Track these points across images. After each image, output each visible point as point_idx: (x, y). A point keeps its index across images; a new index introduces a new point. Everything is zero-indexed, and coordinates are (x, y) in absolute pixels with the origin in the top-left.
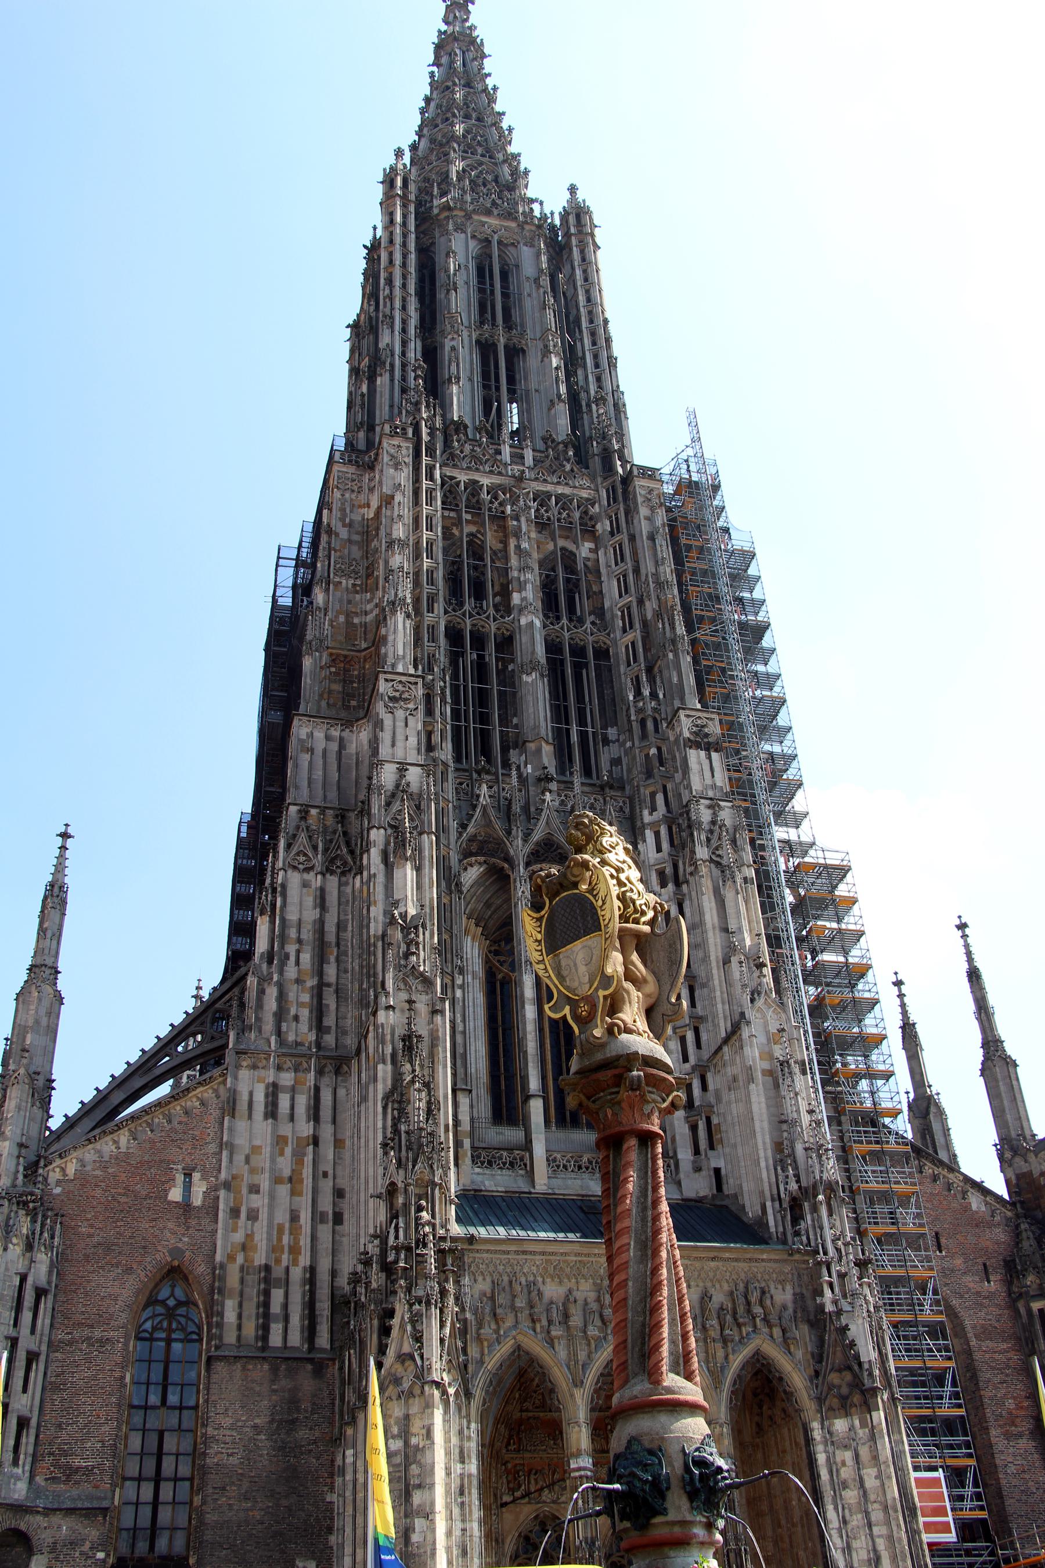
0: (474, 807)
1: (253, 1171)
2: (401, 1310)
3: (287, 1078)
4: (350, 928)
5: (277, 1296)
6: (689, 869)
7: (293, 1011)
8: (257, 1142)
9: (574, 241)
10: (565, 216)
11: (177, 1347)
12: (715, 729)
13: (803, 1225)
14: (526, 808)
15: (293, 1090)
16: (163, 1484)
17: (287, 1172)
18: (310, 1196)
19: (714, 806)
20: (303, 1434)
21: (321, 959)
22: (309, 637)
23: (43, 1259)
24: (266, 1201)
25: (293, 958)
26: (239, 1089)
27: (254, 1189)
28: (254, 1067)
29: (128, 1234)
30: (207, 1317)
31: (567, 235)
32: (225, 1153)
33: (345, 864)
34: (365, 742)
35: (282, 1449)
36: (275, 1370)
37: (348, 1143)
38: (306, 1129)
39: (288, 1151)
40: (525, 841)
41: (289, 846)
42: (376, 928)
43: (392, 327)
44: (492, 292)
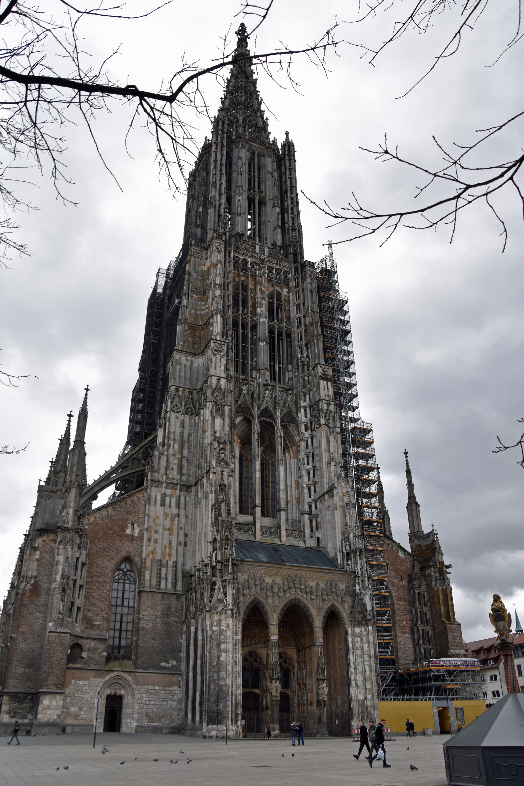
0: (240, 394)
1: (156, 525)
2: (219, 584)
3: (169, 492)
4: (193, 436)
5: (164, 570)
6: (317, 426)
7: (171, 466)
8: (158, 515)
9: (287, 158)
10: (283, 146)
11: (127, 586)
12: (330, 373)
13: (350, 562)
14: (259, 395)
15: (171, 496)
16: (122, 632)
17: (168, 526)
18: (176, 536)
19: (328, 404)
20: (172, 619)
21: (182, 447)
22: (180, 317)
23: (84, 553)
24: (161, 537)
25: (172, 446)
26: (152, 494)
27: (156, 532)
28: (158, 487)
29: (111, 545)
30: (138, 576)
31: (284, 153)
32: (146, 518)
33: (192, 411)
34: (201, 365)
35: (165, 624)
36: (163, 597)
37: (190, 517)
38: (175, 511)
39: (169, 518)
40: (259, 408)
41: (172, 402)
42: (207, 441)
43: (216, 188)
44: (254, 176)
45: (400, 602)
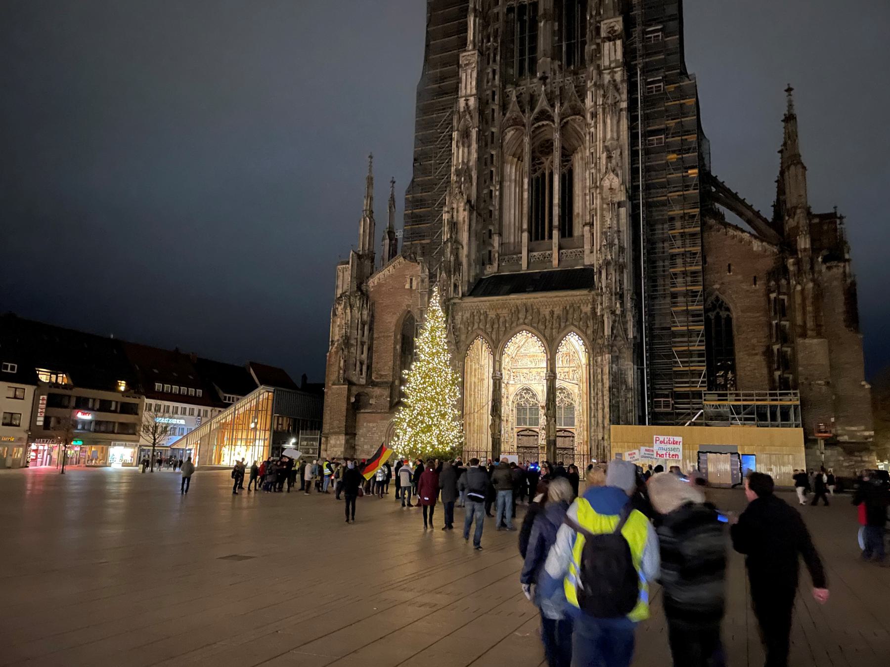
23: (365, 312)
45: (749, 314)
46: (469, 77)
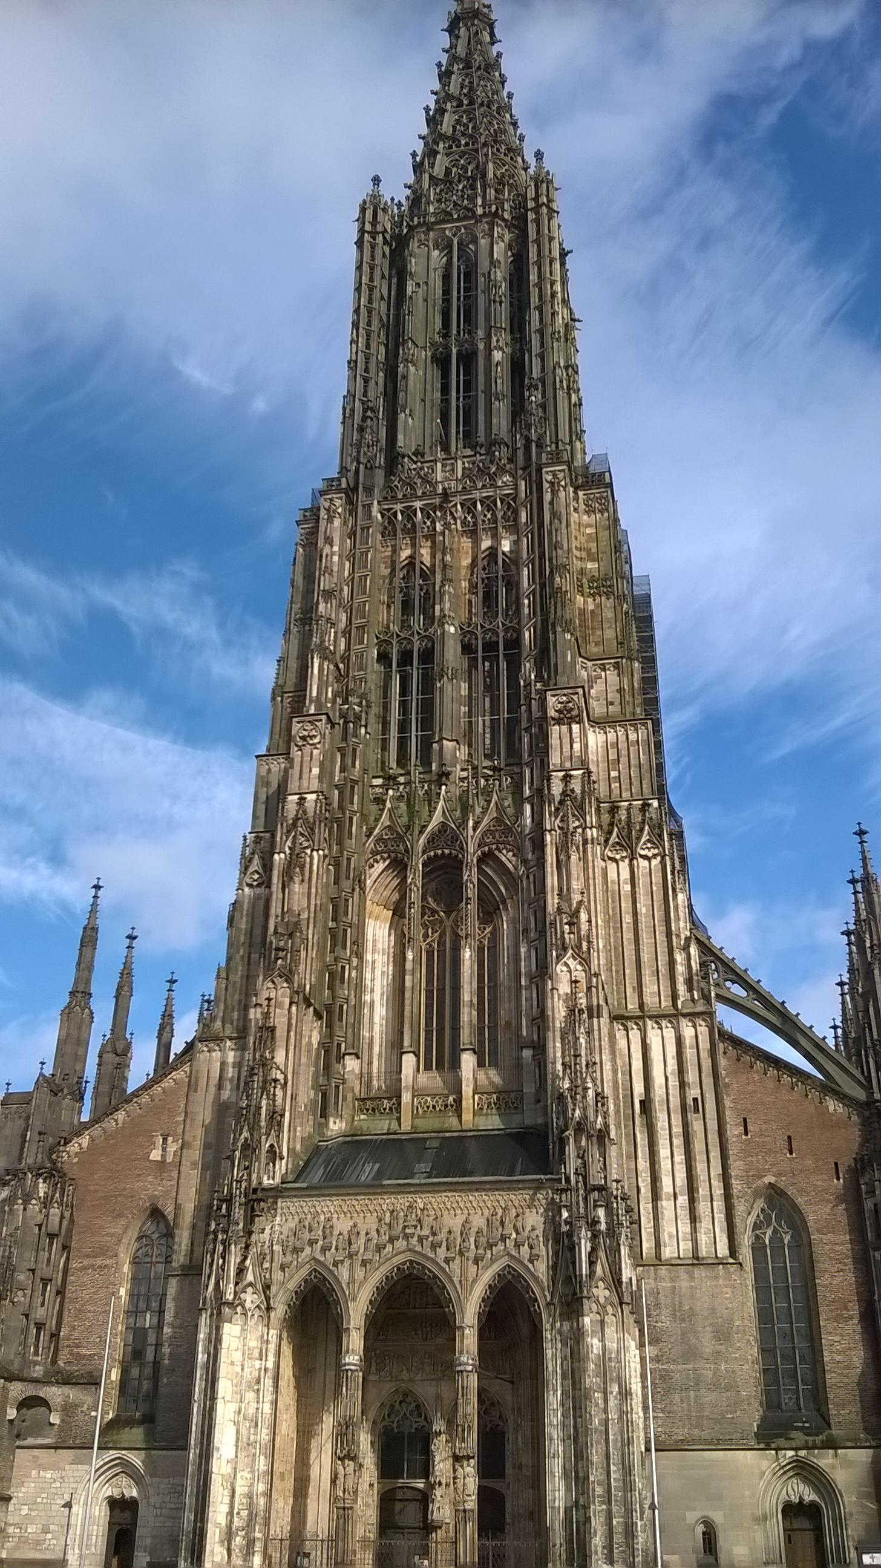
46: (307, 759)
